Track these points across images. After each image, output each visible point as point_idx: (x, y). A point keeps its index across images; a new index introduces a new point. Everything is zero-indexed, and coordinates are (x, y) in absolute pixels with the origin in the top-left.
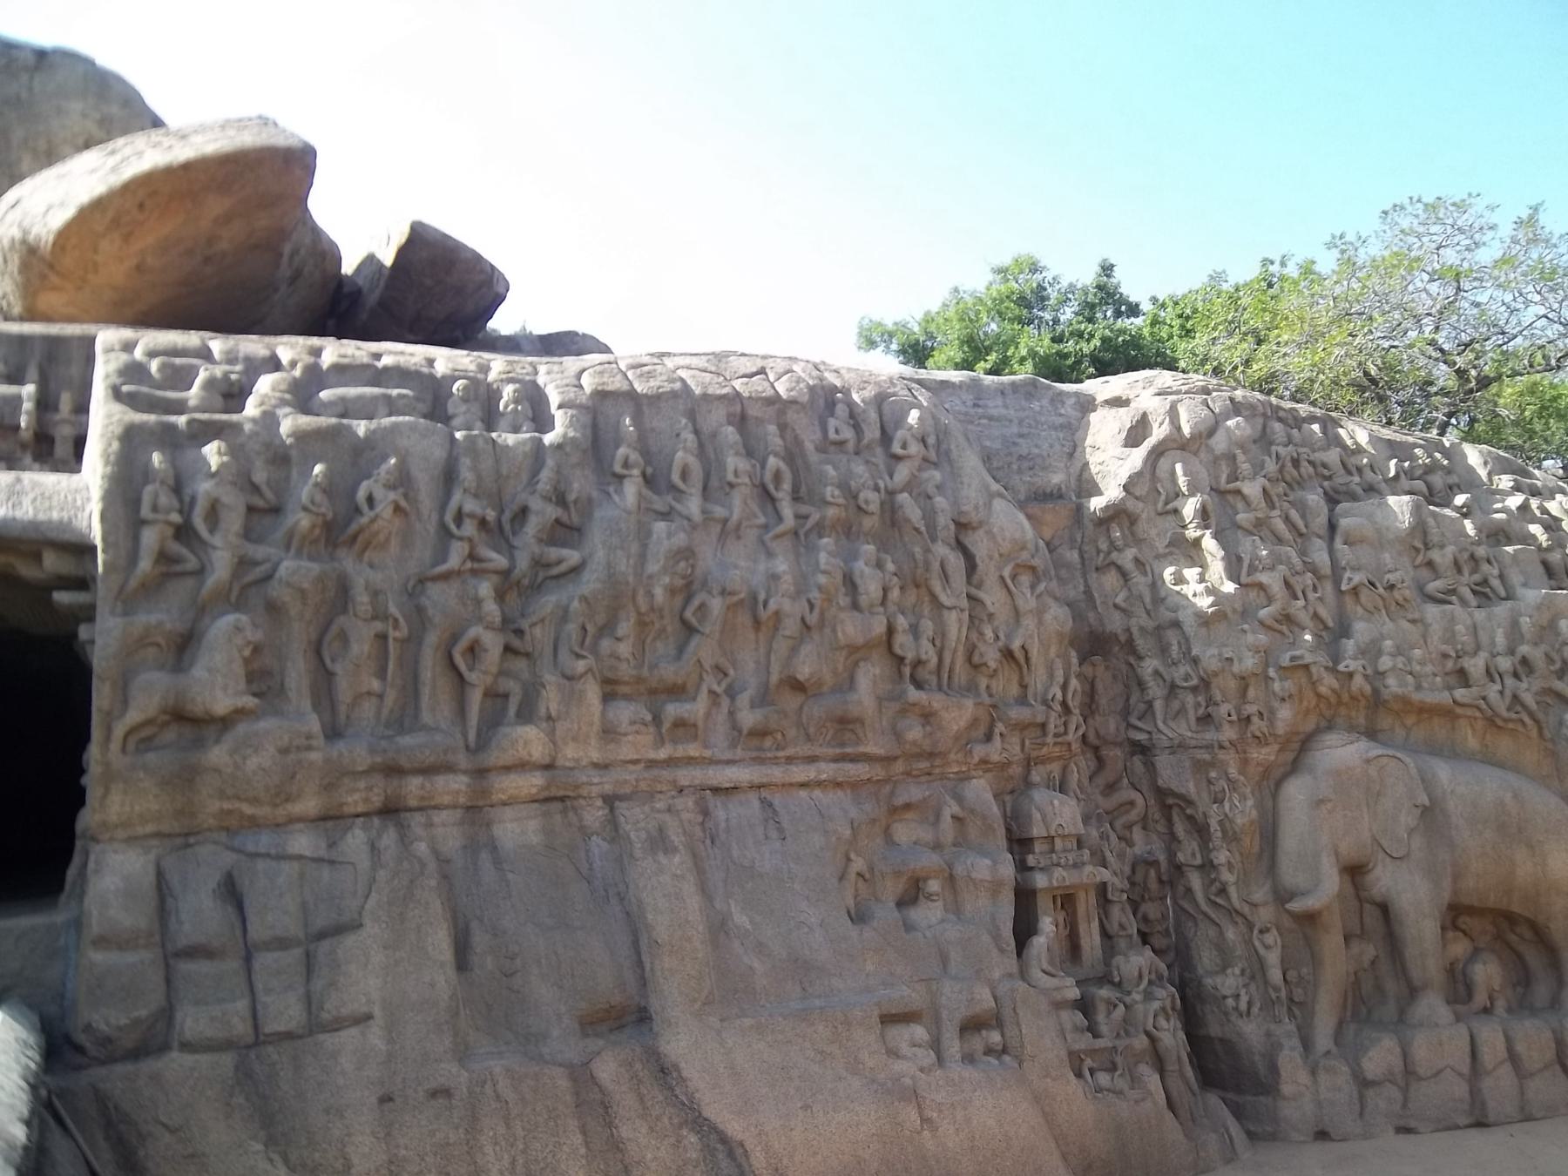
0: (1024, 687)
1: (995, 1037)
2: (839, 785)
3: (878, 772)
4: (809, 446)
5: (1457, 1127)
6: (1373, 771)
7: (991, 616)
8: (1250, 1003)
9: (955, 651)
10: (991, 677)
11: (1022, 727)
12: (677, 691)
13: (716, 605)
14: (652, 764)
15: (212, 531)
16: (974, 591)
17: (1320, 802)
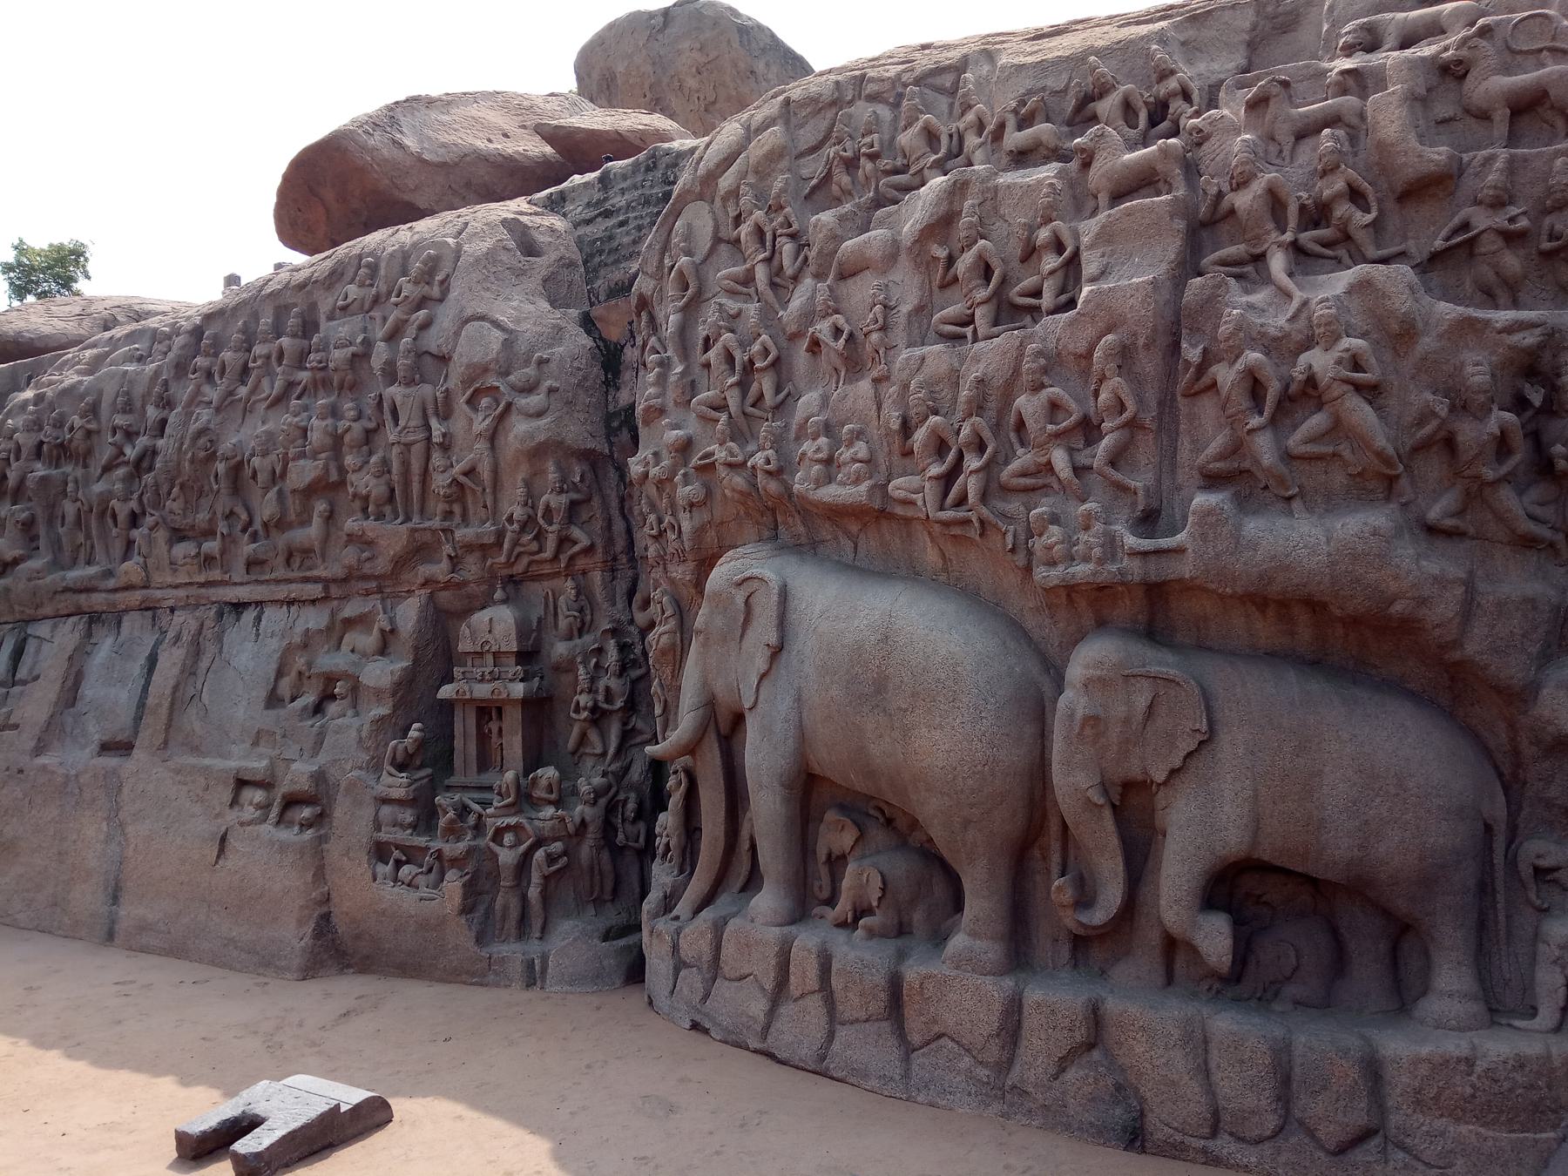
0: (485, 506)
1: (307, 812)
2: (313, 602)
3: (335, 591)
4: (323, 319)
5: (747, 1049)
6: (740, 600)
7: (441, 445)
8: (668, 848)
9: (406, 483)
10: (450, 503)
11: (484, 549)
12: (209, 533)
13: (221, 467)
14: (202, 585)
15: (17, 459)
16: (434, 423)
17: (699, 632)
